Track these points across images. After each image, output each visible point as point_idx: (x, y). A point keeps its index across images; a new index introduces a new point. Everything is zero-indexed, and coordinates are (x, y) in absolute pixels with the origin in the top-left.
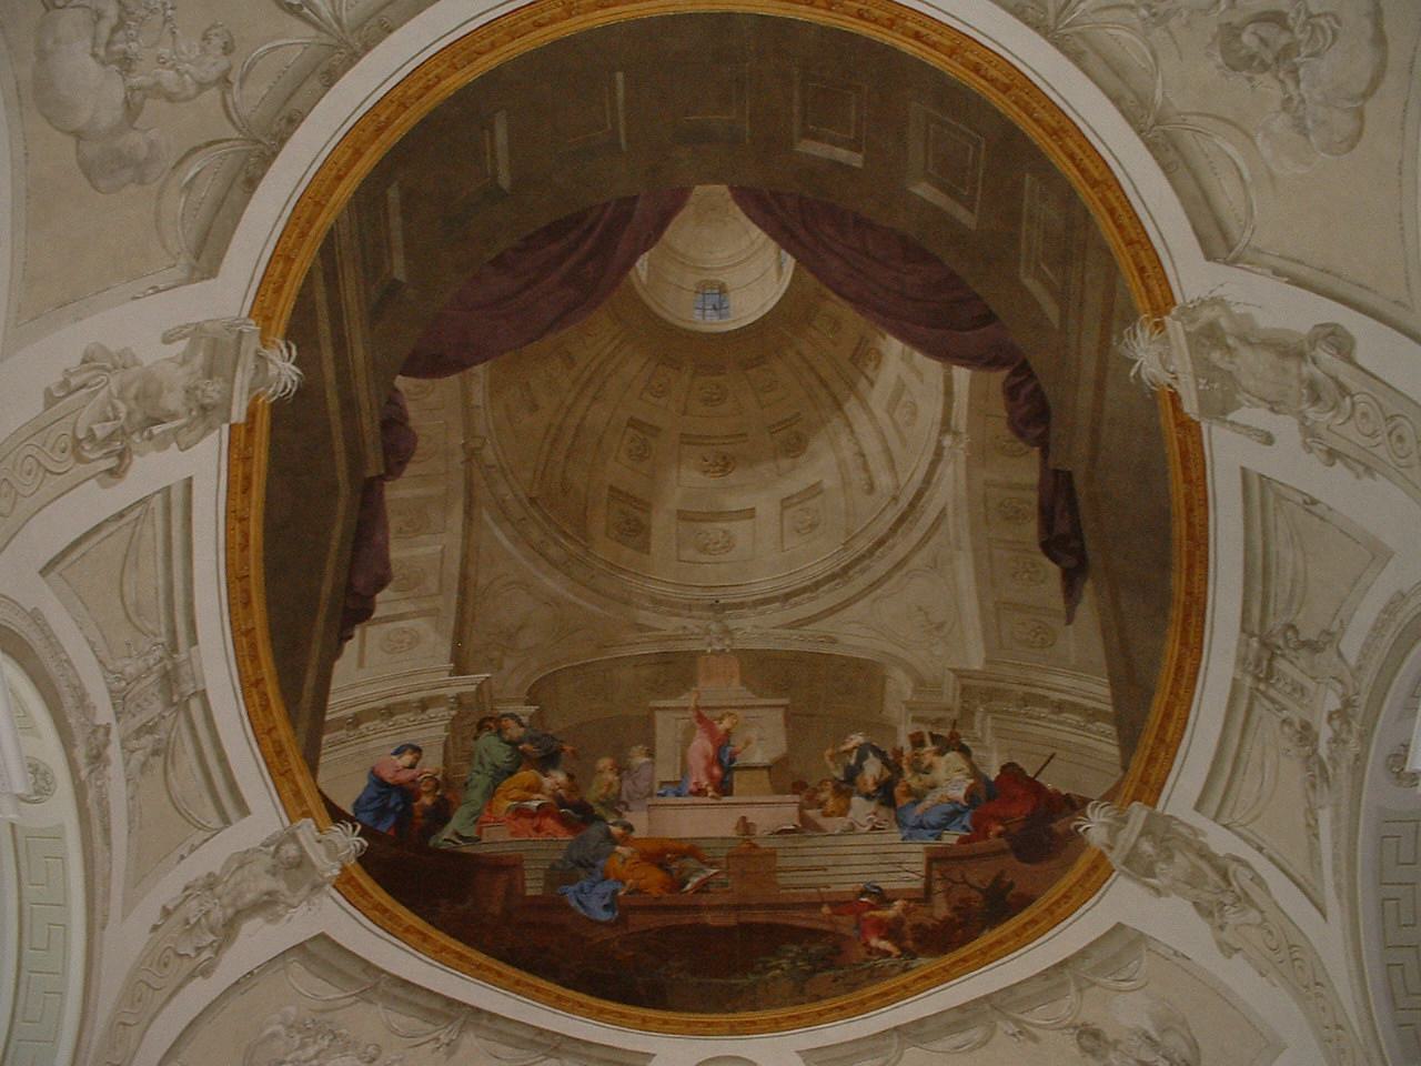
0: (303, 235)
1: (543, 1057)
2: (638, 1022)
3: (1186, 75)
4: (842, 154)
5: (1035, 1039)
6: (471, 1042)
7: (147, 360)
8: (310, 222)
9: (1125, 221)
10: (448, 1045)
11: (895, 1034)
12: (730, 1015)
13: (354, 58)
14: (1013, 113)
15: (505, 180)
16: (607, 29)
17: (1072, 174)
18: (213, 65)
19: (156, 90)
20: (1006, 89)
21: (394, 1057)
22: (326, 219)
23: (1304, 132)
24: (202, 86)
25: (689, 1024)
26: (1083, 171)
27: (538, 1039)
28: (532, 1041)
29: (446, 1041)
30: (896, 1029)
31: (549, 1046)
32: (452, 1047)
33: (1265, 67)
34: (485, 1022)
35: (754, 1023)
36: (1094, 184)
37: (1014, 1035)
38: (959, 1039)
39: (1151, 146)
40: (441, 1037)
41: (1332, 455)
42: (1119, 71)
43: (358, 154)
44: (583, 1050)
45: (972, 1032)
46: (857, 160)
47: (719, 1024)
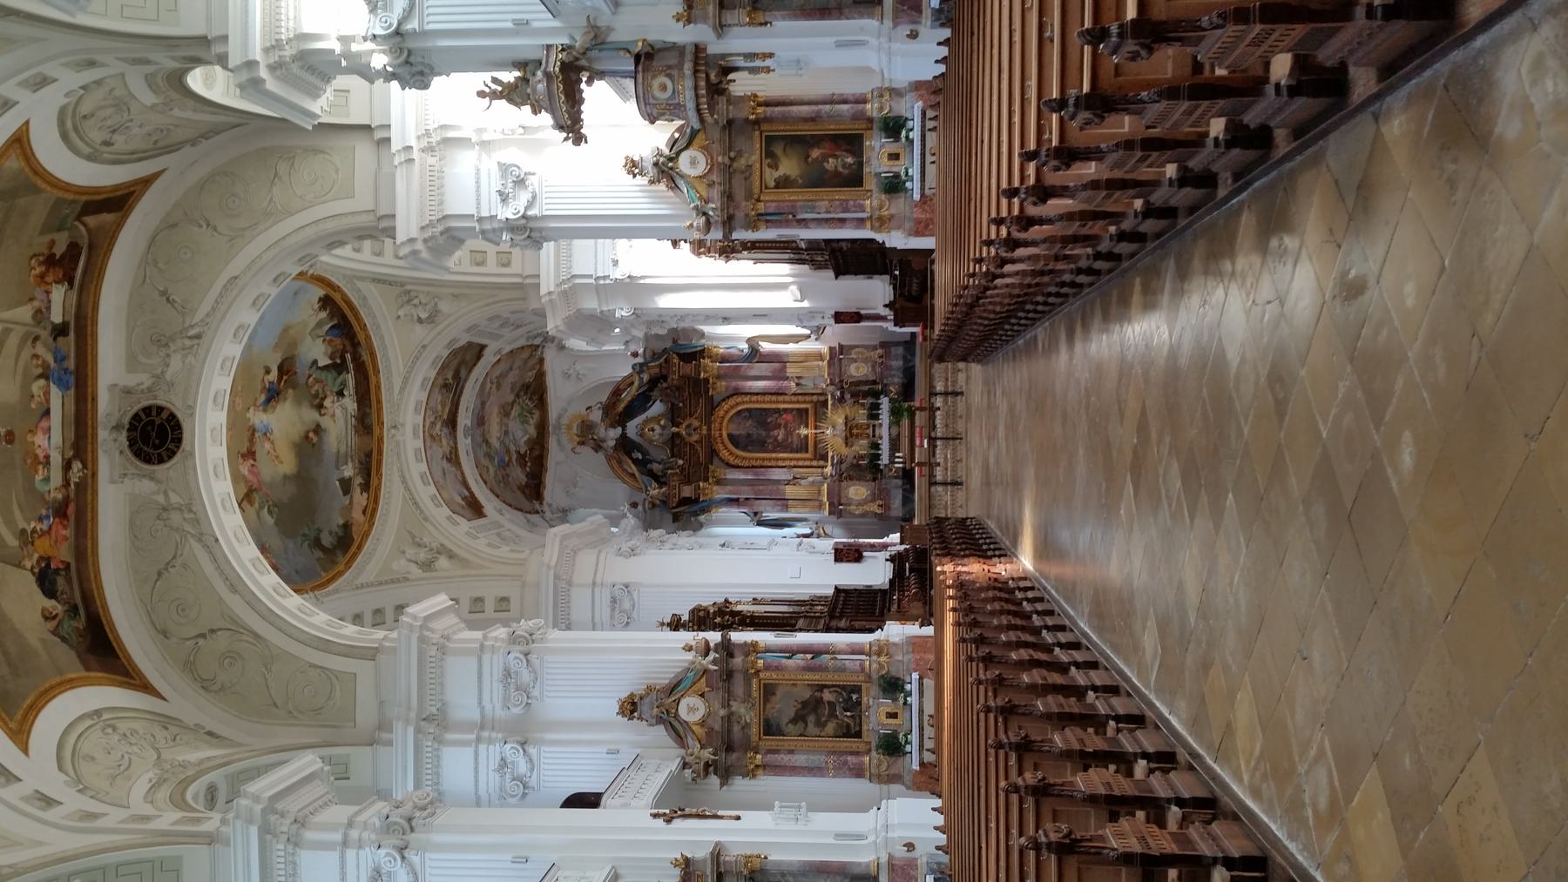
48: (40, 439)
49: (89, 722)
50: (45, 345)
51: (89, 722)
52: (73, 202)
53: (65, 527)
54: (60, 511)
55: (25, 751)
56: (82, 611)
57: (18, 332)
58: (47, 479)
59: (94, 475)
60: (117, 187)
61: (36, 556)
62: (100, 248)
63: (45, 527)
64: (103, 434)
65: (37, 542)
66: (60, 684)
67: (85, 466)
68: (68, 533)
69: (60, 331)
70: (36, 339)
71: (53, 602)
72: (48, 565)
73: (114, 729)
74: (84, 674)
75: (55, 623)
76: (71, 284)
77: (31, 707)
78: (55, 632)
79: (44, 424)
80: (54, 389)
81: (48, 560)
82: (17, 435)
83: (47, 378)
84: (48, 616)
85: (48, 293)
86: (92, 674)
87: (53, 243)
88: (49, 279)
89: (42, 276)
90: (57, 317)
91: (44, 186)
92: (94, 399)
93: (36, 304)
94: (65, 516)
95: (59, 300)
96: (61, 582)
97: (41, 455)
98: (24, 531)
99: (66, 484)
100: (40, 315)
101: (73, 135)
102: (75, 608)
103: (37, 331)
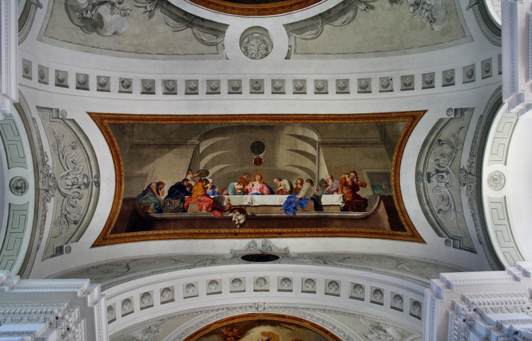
1: (185, 27)
2: (223, 8)
5: (372, 8)
6: (158, 13)
10: (150, 12)
11: (320, 17)
12: (258, 5)
21: (128, 7)
25: (242, 9)
27: (185, 17)
28: (182, 19)
29: (149, 10)
30: (320, 15)
31: (188, 21)
32: (151, 14)
34: (165, 5)
35: (266, 9)
37: (365, 10)
38: (344, 18)
40: (148, 7)
44: (201, 23)
45: (349, 13)
47: (253, 10)
48: (257, 186)
49: (94, 173)
50: (309, 190)
51: (94, 173)
52: (390, 186)
53: (207, 208)
54: (216, 205)
55: (90, 114)
56: (158, 216)
57: (315, 171)
58: (235, 193)
59: (236, 235)
60: (404, 213)
61: (193, 183)
62: (366, 228)
63: (209, 191)
64: (259, 242)
65: (200, 185)
66: (121, 175)
67: (242, 226)
68: (204, 213)
69: (318, 206)
70: (311, 182)
71: (166, 194)
72: (187, 193)
73: (86, 185)
74: (122, 197)
75: (155, 191)
76: (344, 209)
77: (112, 142)
78: (149, 187)
79: (266, 190)
80: (284, 198)
81: (190, 194)
82: (260, 167)
83: (290, 192)
84: (160, 185)
85: (337, 191)
86: (121, 201)
87: (364, 185)
88: (345, 191)
89: (345, 184)
90: (326, 200)
91: (394, 158)
92: (280, 235)
93: (330, 182)
94: (214, 209)
95: (333, 200)
96: (177, 203)
97: (248, 187)
98: (207, 173)
99: (232, 209)
100: (323, 184)
101: (427, 148)
102: (160, 211)
103: (316, 184)
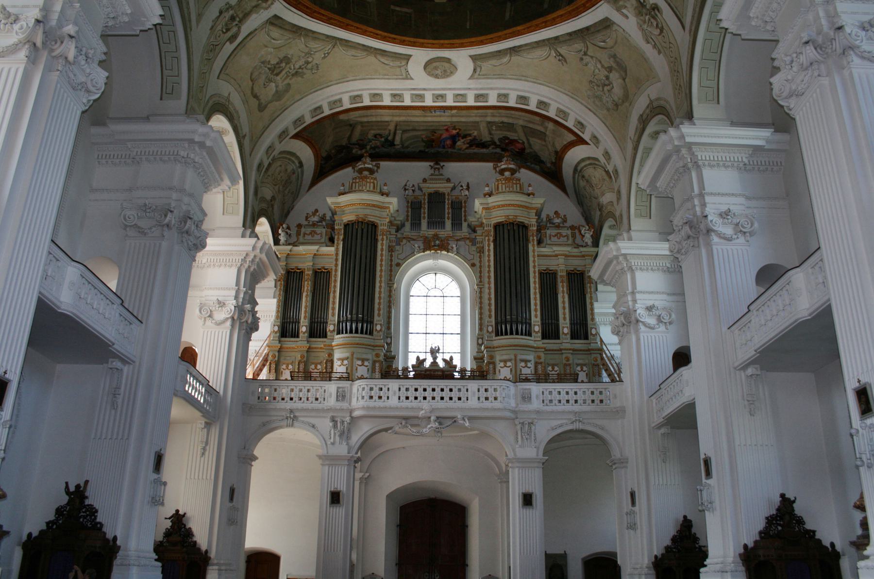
0: (577, 8)
3: (297, 47)
4: (398, 9)
7: (635, 19)
8: (573, 10)
9: (302, 7)
13: (548, 40)
14: (344, 20)
15: (509, 4)
16: (471, 37)
17: (322, 11)
18: (587, 59)
19: (603, 66)
20: (348, 25)
22: (569, 8)
23: (263, 63)
24: (592, 57)
26: (319, 13)
33: (277, 63)
36: (315, 12)
39: (300, 28)
41: (221, 12)
42: (315, 39)
43: (554, 19)
46: (392, 7)
